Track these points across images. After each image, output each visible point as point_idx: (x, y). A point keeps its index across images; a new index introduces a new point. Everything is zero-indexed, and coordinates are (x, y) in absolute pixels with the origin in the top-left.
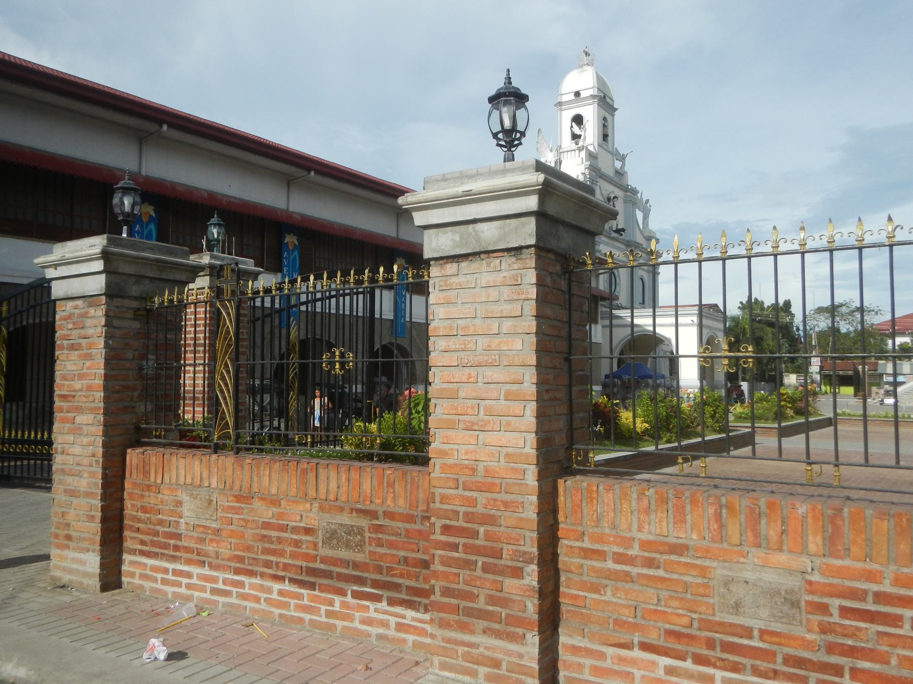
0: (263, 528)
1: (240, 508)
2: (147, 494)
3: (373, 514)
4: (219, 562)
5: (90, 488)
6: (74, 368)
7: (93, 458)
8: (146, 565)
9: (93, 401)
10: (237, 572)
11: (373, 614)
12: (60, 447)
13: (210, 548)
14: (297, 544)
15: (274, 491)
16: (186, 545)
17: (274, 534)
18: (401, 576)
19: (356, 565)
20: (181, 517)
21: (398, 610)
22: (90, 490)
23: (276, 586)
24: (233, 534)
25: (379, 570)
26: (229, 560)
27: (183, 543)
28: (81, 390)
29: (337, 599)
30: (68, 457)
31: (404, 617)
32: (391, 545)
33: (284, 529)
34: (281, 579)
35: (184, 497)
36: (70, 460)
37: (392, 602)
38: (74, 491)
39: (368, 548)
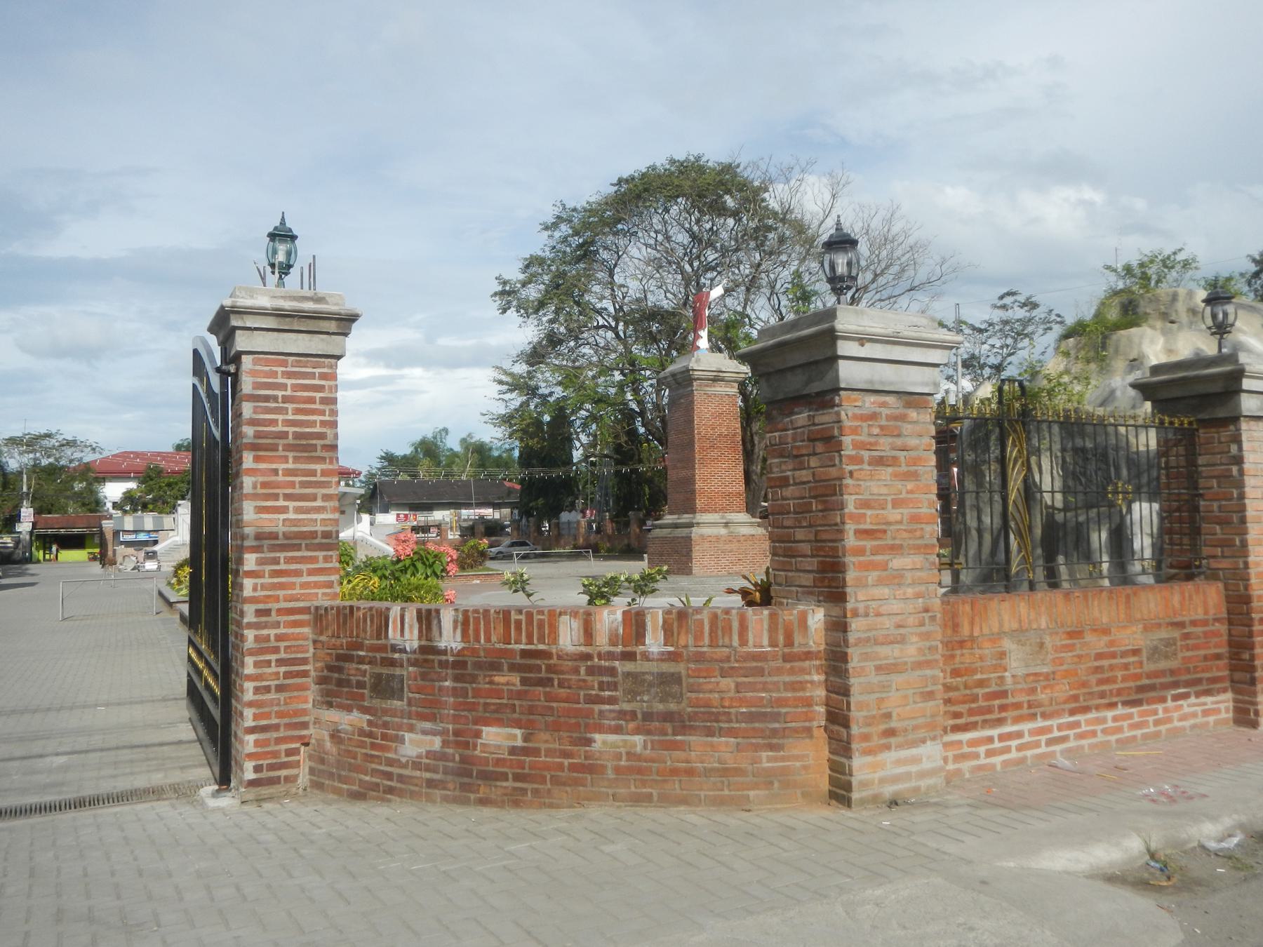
0: (1096, 659)
1: (1074, 645)
2: (958, 652)
3: (1181, 625)
4: (1055, 707)
5: (924, 655)
6: (884, 491)
7: (924, 614)
8: (960, 742)
9: (922, 537)
10: (1073, 712)
11: (1187, 710)
12: (861, 607)
13: (1042, 696)
14: (1126, 667)
15: (1105, 620)
16: (1014, 700)
17: (1106, 663)
18: (1203, 671)
19: (1172, 672)
20: (1006, 670)
21: (1203, 699)
22: (924, 658)
23: (1110, 714)
24: (1067, 674)
25: (1188, 671)
26: (1065, 702)
27: (1010, 700)
28: (901, 522)
29: (1160, 707)
30: (879, 619)
31: (1205, 704)
32: (1196, 647)
33: (1113, 655)
34: (1112, 705)
35: (1007, 644)
36: (888, 623)
37: (1198, 695)
38: (894, 665)
39: (1180, 655)
